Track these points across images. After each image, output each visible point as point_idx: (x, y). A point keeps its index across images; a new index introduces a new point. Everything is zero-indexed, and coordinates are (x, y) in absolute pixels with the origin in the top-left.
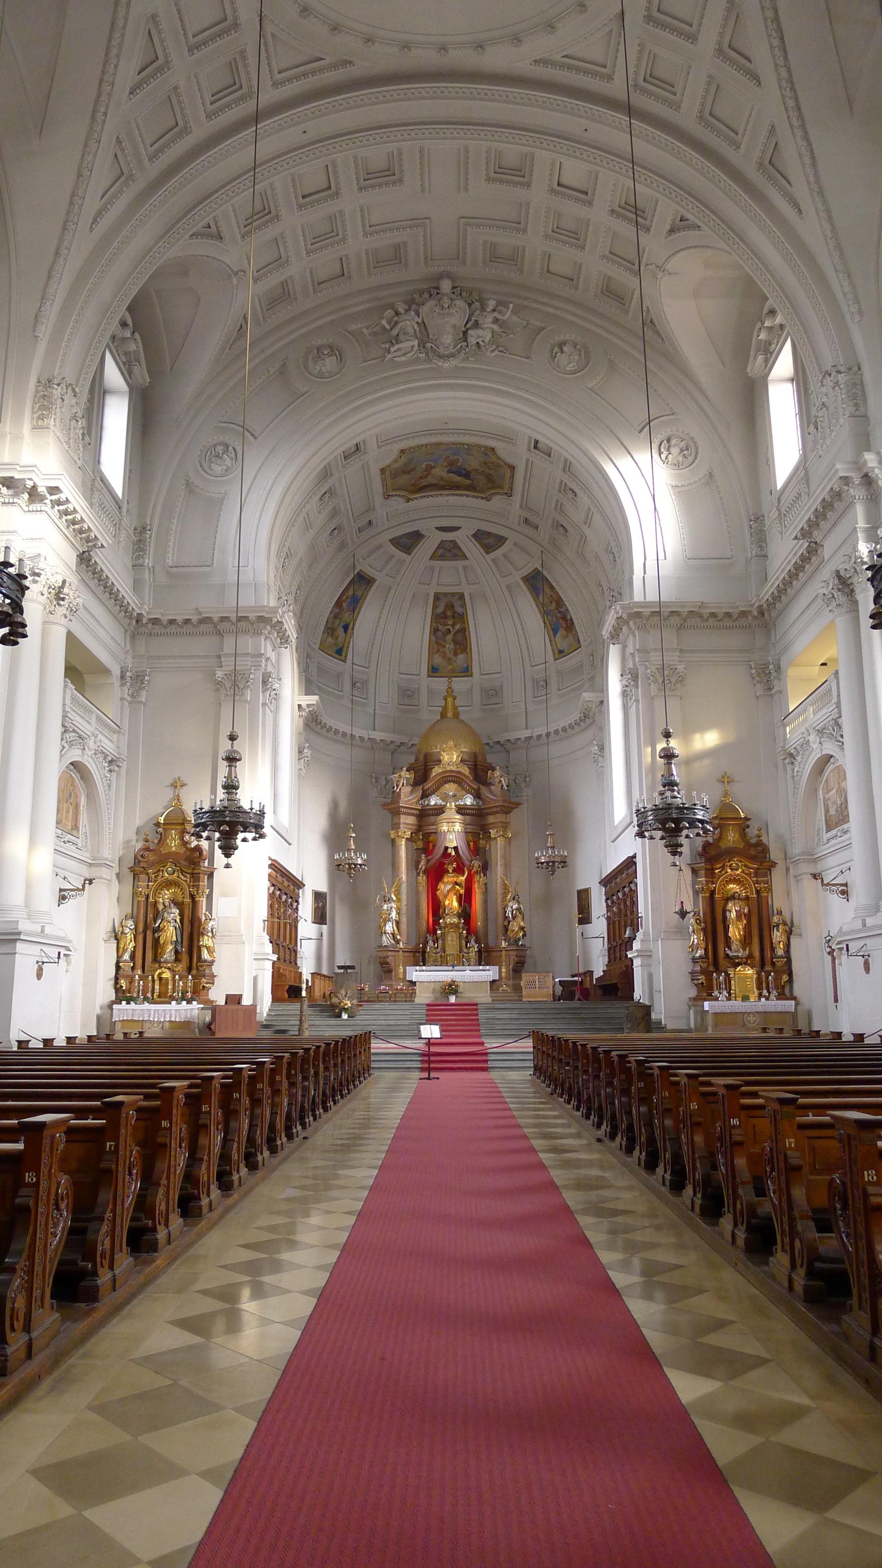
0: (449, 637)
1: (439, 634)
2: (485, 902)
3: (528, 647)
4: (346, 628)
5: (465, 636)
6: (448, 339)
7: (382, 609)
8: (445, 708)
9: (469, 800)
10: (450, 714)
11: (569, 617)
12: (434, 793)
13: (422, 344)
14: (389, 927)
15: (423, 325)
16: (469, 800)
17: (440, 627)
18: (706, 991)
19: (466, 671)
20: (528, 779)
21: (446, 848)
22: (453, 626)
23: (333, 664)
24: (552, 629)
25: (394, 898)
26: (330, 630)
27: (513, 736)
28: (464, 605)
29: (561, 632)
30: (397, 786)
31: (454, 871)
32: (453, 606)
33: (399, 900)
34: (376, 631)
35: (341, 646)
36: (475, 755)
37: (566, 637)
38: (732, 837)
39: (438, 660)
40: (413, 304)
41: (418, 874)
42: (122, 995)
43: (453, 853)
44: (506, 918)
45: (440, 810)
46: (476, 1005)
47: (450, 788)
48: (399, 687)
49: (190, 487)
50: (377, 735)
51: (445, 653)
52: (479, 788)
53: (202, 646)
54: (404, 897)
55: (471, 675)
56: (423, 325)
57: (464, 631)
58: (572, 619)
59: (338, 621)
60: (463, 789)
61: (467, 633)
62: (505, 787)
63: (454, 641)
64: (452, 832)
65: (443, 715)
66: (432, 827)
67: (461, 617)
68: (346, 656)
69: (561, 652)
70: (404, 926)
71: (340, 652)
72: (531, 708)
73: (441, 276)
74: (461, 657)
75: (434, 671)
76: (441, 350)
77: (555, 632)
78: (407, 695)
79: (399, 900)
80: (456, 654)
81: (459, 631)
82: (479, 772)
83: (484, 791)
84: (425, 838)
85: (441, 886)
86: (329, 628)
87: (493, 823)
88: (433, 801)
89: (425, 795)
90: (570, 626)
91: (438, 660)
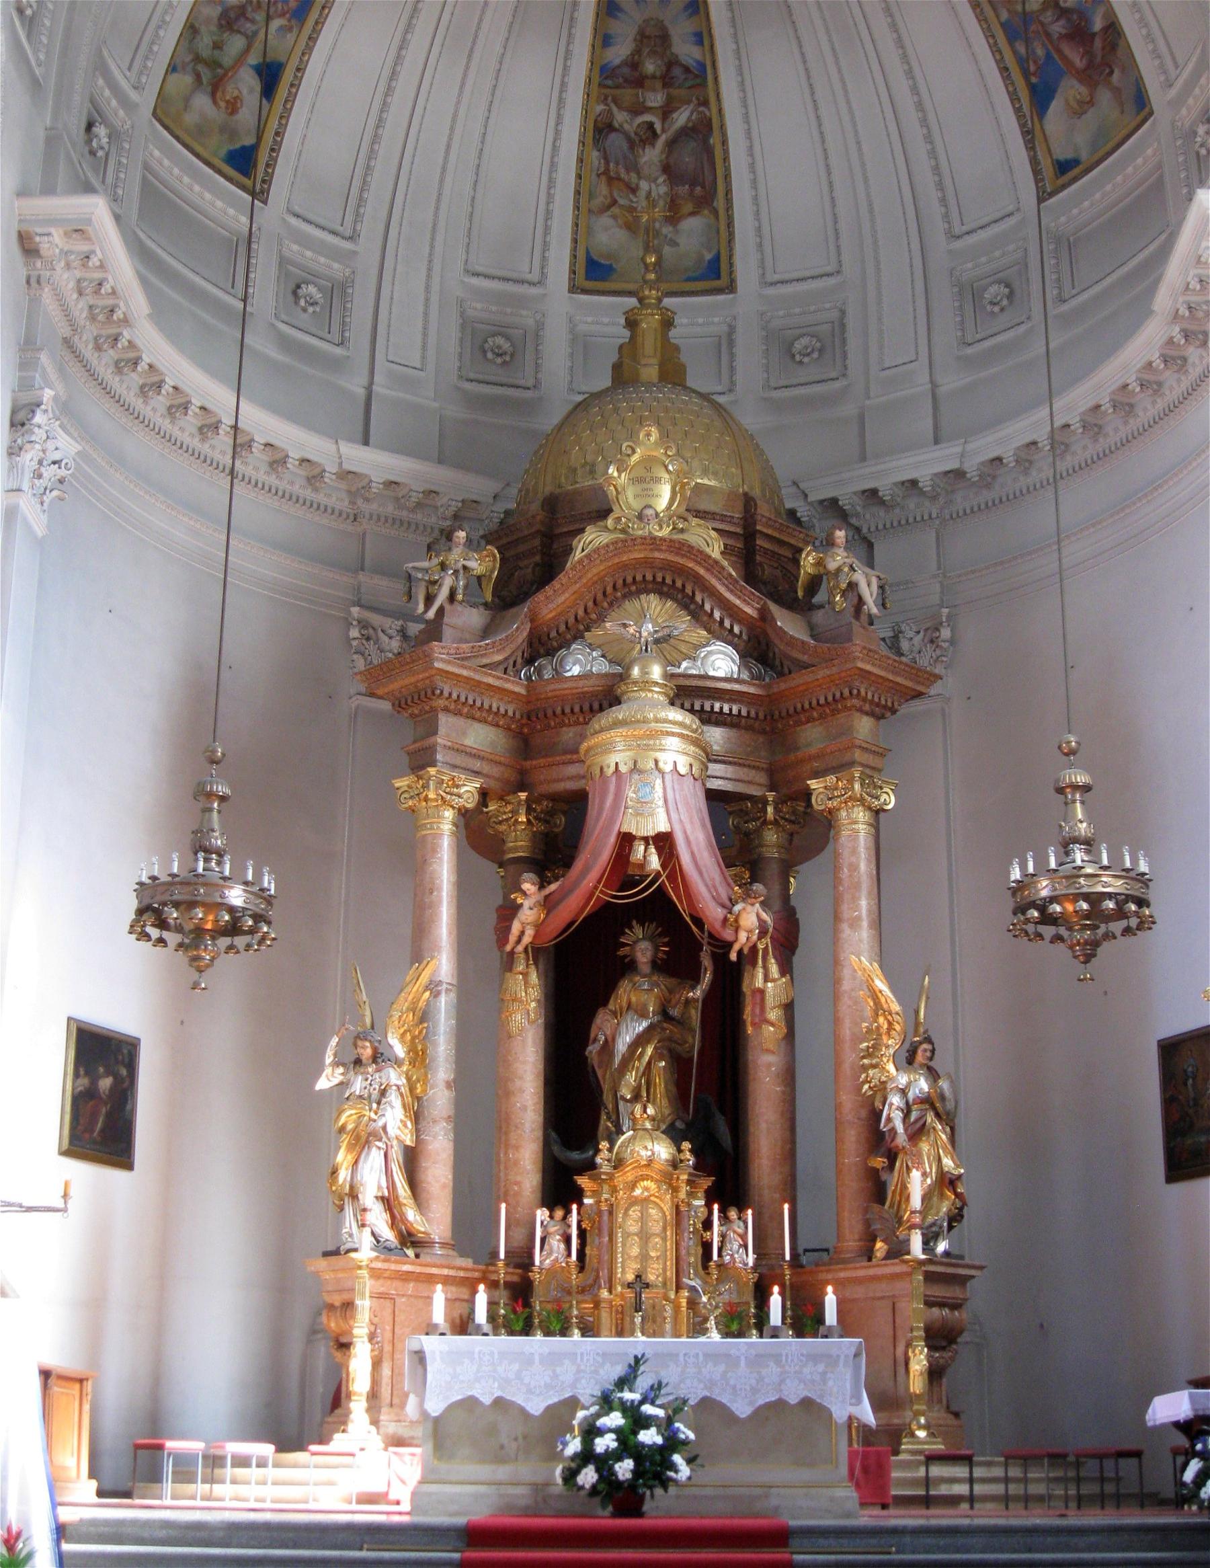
0: (652, 156)
1: (615, 142)
2: (789, 1076)
3: (936, 169)
4: (270, 77)
5: (709, 151)
7: (409, 28)
8: (629, 351)
10: (650, 372)
11: (1098, 25)
12: (578, 636)
14: (373, 1174)
16: (721, 663)
17: (620, 117)
19: (714, 274)
20: (946, 633)
21: (627, 840)
22: (666, 112)
23: (217, 200)
24: (1033, 89)
25: (400, 1051)
26: (201, 64)
27: (887, 474)
28: (703, 37)
29: (1070, 90)
30: (429, 600)
31: (658, 966)
32: (664, 38)
33: (419, 1057)
34: (385, 106)
35: (249, 141)
37: (1081, 108)
39: (609, 236)
41: (509, 962)
43: (654, 862)
44: (877, 1139)
45: (607, 696)
46: (779, 1537)
47: (651, 616)
48: (466, 324)
50: (375, 463)
51: (632, 210)
52: (764, 614)
54: (443, 1047)
55: (731, 288)
57: (704, 133)
58: (1113, 29)
59: (236, 44)
60: (697, 614)
61: (715, 140)
62: (871, 606)
63: (666, 169)
65: (623, 376)
66: (572, 770)
67: (697, 81)
68: (267, 181)
69: (1065, 167)
70: (439, 1173)
71: (245, 164)
72: (950, 382)
74: (693, 227)
75: (594, 272)
77: (1041, 97)
78: (496, 349)
79: (419, 1057)
80: (674, 218)
81: (685, 132)
82: (766, 554)
83: (787, 623)
84: (539, 814)
85: (602, 1023)
86: (197, 59)
87: (819, 756)
88: (579, 665)
89: (543, 646)
91: (609, 236)
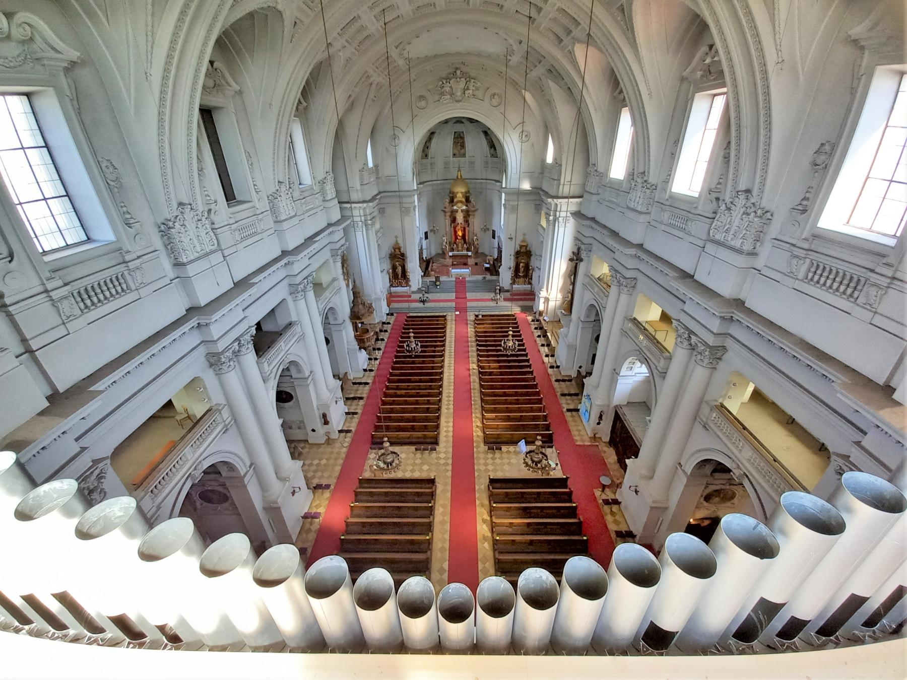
6: (459, 94)
9: (464, 207)
13: (452, 94)
15: (451, 87)
16: (464, 207)
18: (514, 283)
19: (464, 155)
23: (425, 161)
26: (423, 151)
36: (466, 193)
38: (523, 250)
39: (456, 152)
40: (448, 79)
42: (391, 286)
45: (457, 211)
47: (460, 205)
49: (387, 149)
53: (397, 200)
56: (451, 87)
64: (460, 218)
67: (463, 138)
73: (457, 69)
74: (462, 151)
76: (457, 98)
78: (446, 165)
88: (455, 208)
90: (495, 149)
